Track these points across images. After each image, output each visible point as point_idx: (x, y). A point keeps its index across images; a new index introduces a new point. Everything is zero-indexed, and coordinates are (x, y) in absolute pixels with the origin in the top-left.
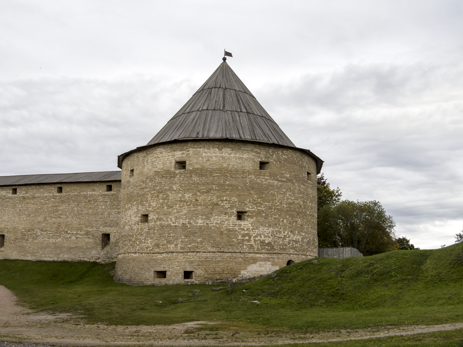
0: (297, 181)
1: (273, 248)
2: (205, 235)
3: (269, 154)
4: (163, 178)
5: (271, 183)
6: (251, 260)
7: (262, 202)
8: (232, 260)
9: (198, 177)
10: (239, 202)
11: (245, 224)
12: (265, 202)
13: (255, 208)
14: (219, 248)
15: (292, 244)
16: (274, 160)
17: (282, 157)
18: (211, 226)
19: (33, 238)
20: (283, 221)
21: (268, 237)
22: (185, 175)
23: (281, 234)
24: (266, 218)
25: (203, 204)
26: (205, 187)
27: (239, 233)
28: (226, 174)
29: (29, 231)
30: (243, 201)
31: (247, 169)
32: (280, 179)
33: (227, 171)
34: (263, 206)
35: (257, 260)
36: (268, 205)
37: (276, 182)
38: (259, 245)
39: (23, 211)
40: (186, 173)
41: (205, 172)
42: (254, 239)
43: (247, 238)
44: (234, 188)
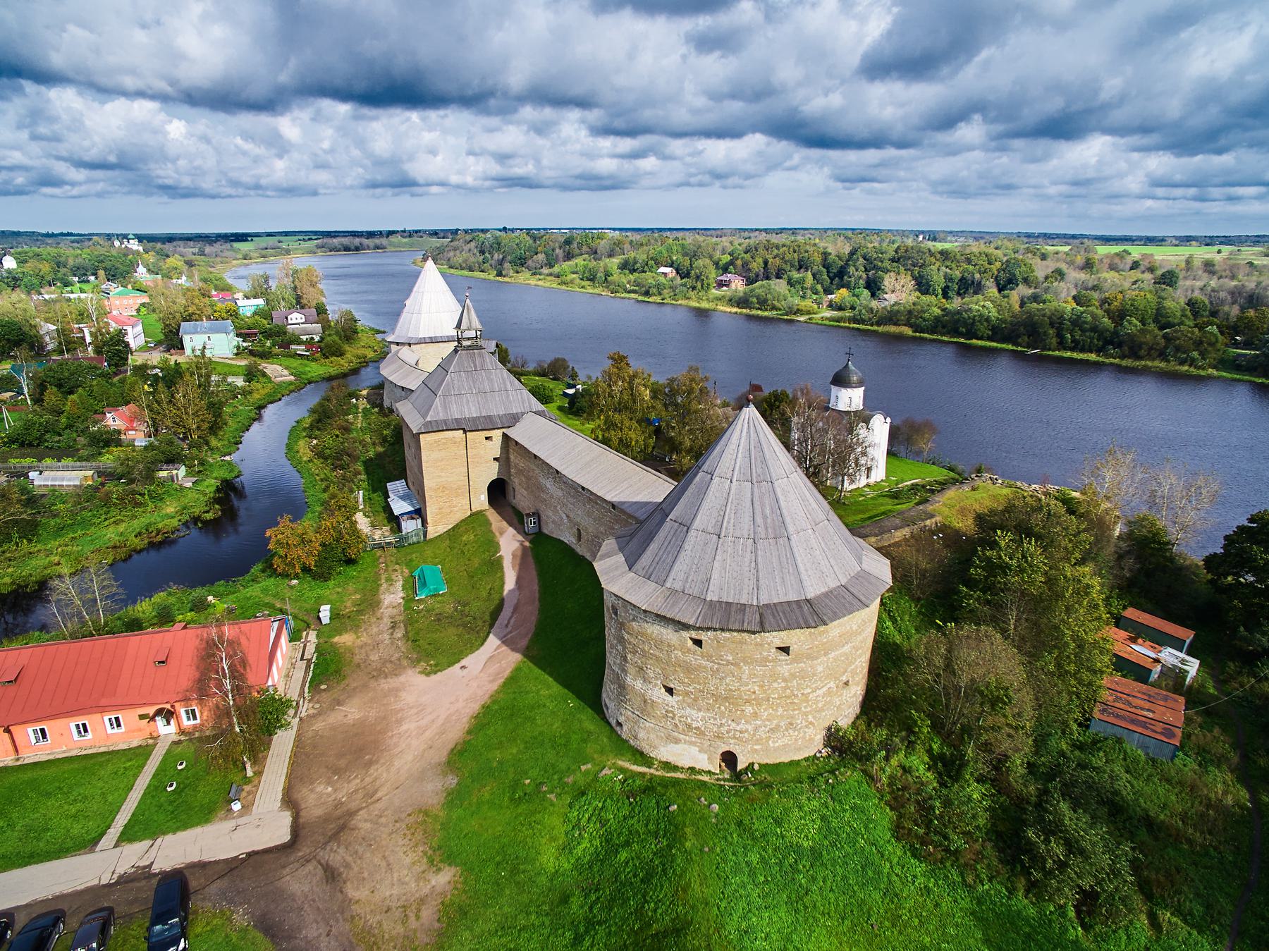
0: (746, 663)
1: (703, 733)
20: (719, 708)
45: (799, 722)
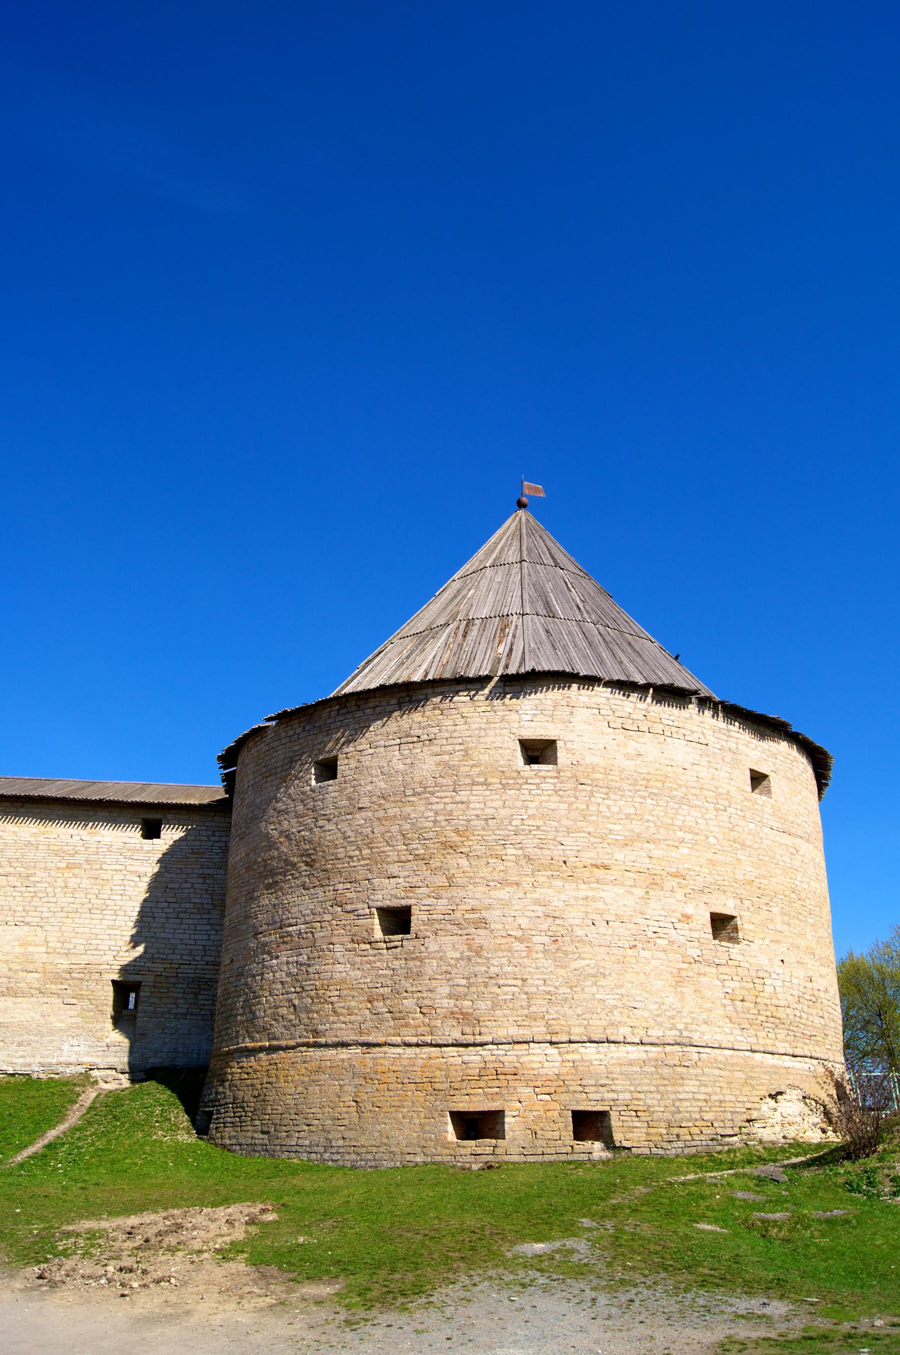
2: (632, 983)
4: (474, 788)
14: (677, 1029)
26: (619, 827)
41: (618, 779)
44: (698, 837)
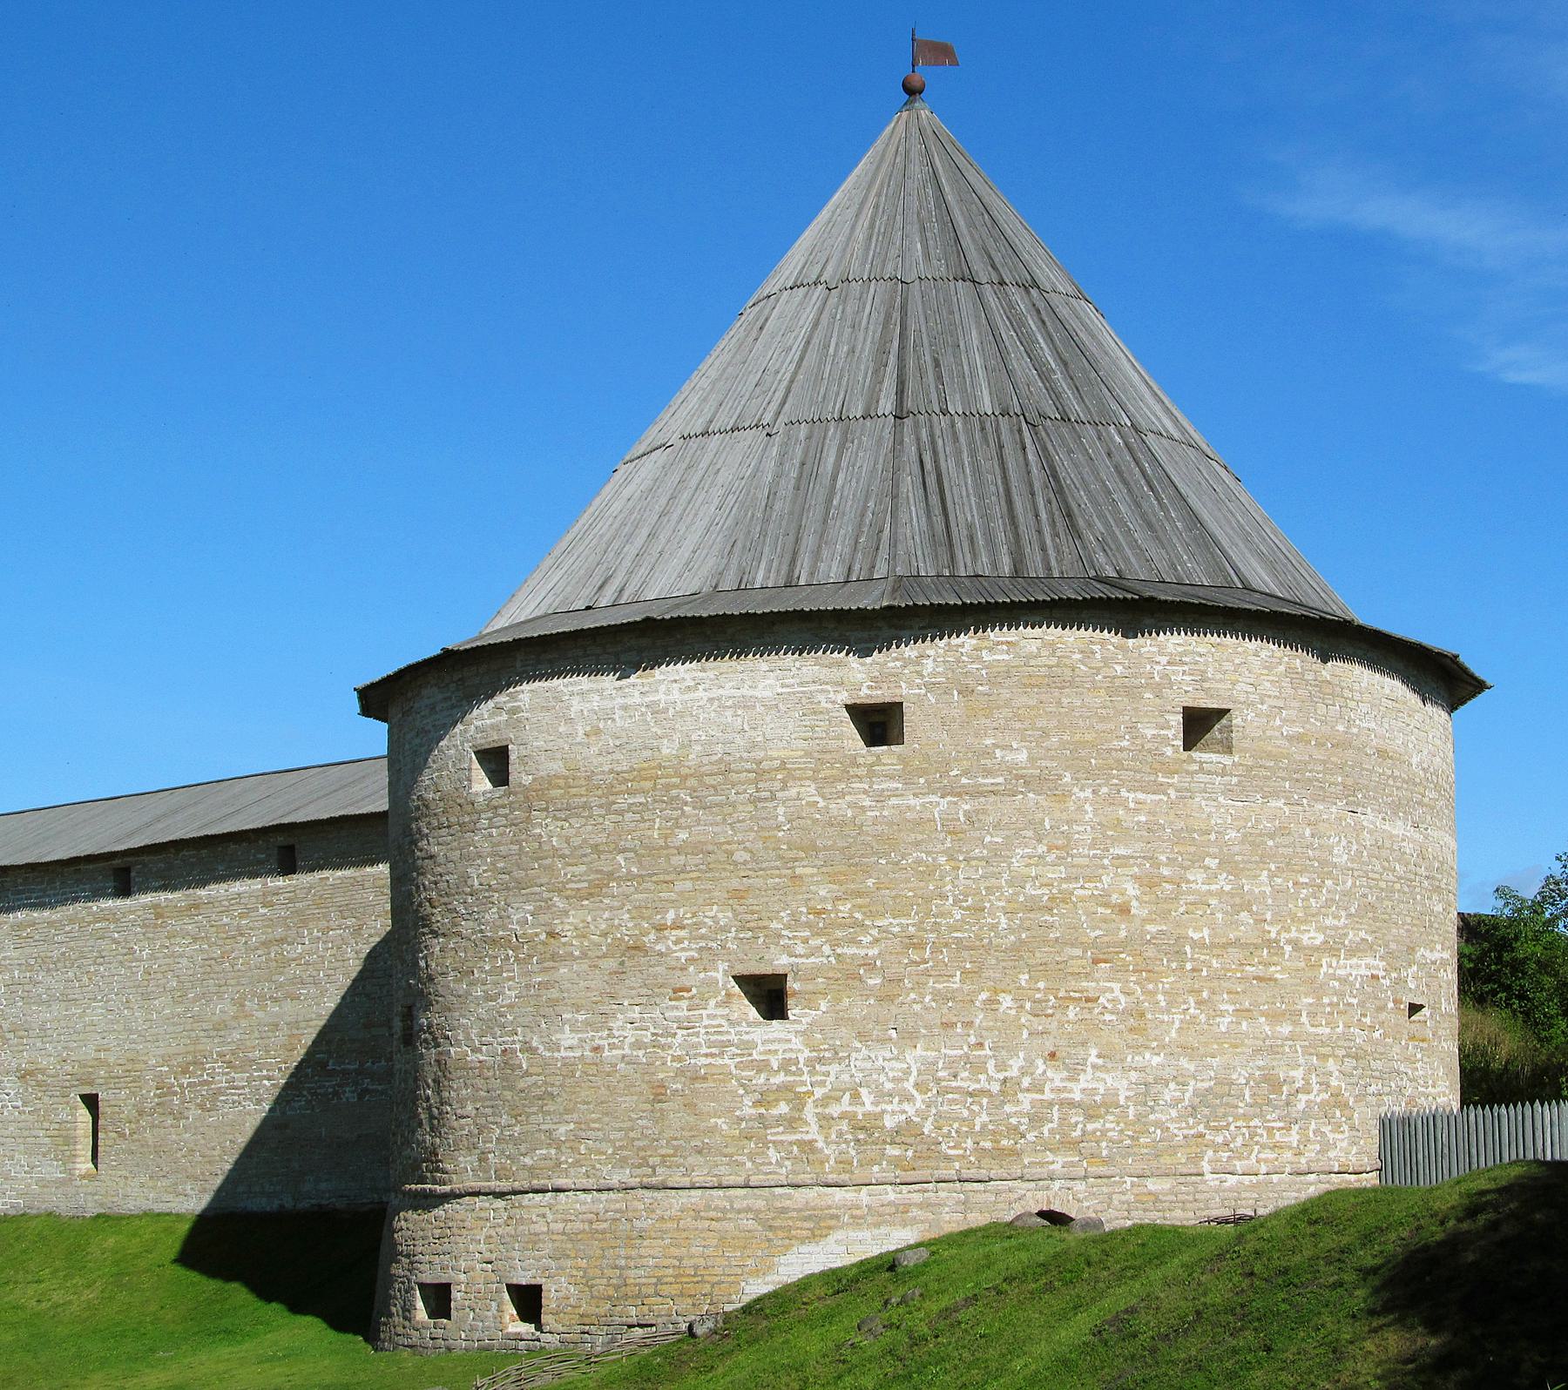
1: (930, 1150)
2: (588, 1103)
3: (897, 660)
5: (909, 808)
6: (799, 1224)
7: (858, 915)
8: (707, 1223)
9: (555, 818)
10: (742, 929)
11: (771, 1036)
12: (871, 915)
13: (827, 949)
14: (648, 1166)
15: (1060, 1125)
16: (930, 687)
17: (980, 658)
18: (614, 1061)
19: (201, 1106)
20: (992, 1002)
21: (897, 1098)
22: (505, 816)
23: (982, 1077)
24: (886, 998)
25: (577, 953)
26: (583, 868)
27: (742, 1085)
28: (674, 792)
29: (184, 1073)
30: (761, 924)
31: (775, 754)
32: (964, 781)
33: (680, 776)
34: (870, 939)
35: (833, 1222)
36: (897, 929)
37: (944, 802)
38: (846, 1141)
39: (160, 976)
40: (512, 803)
42: (819, 1110)
43: (783, 1108)
45: (1298, 1074)
